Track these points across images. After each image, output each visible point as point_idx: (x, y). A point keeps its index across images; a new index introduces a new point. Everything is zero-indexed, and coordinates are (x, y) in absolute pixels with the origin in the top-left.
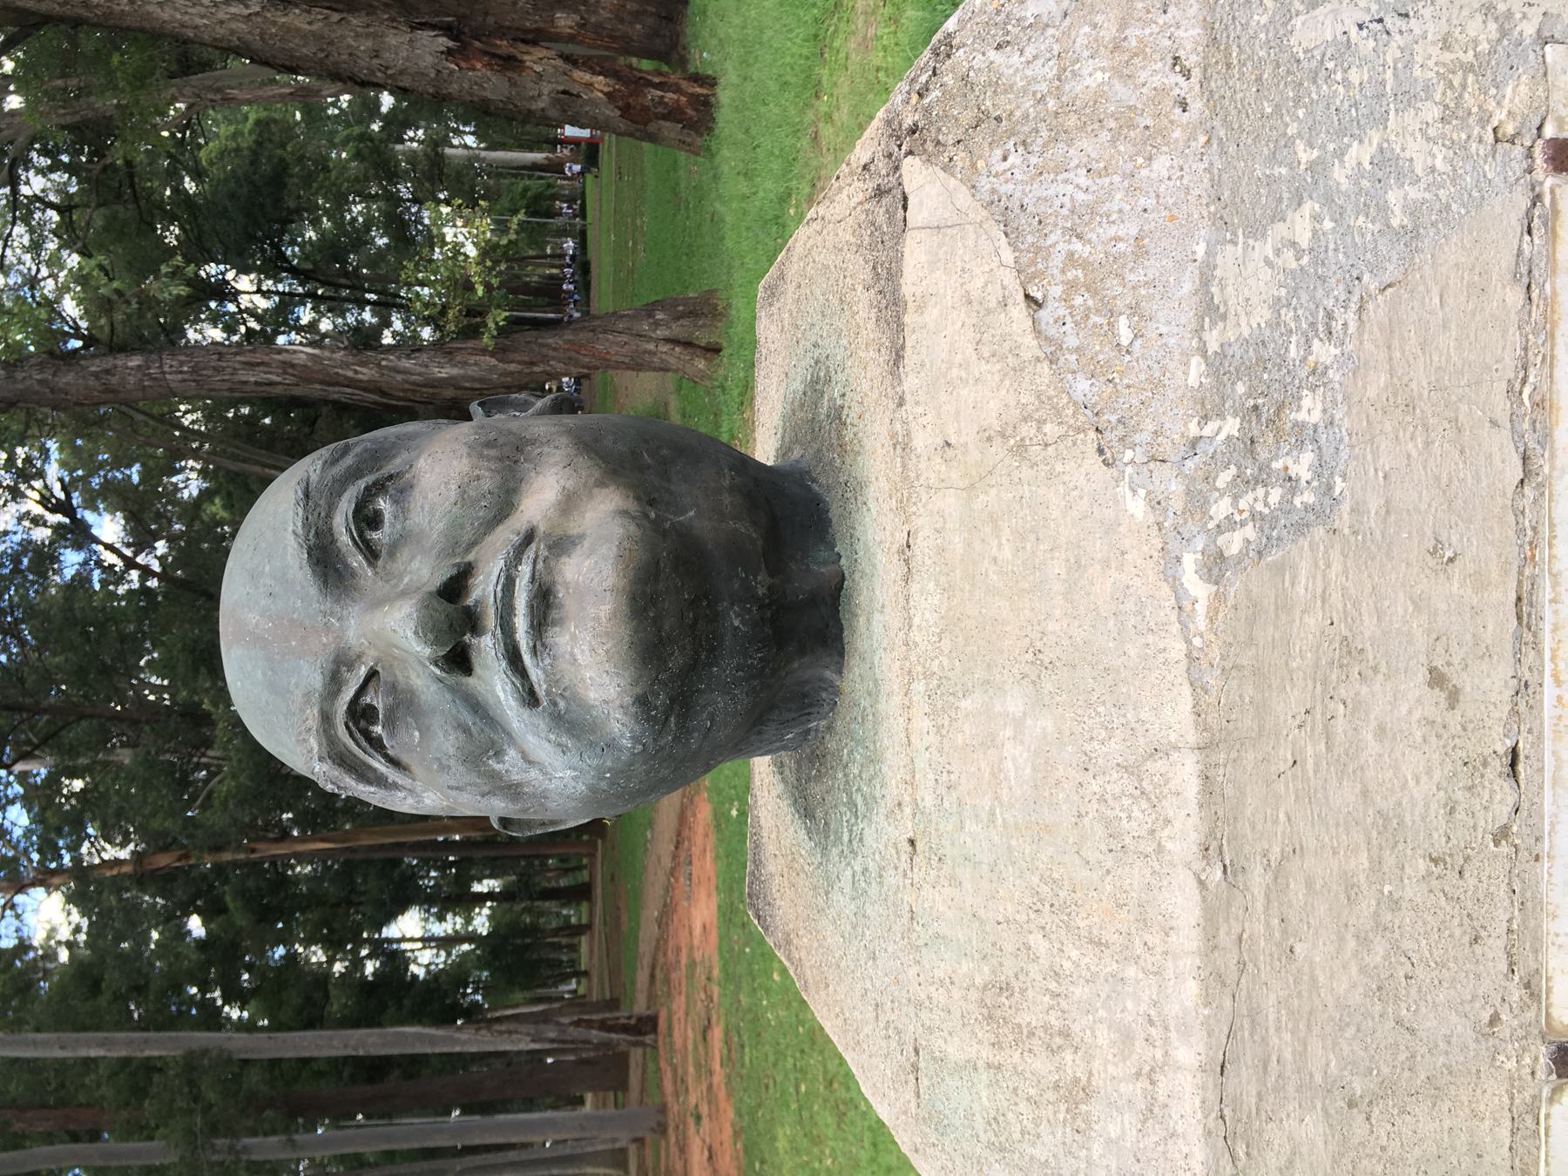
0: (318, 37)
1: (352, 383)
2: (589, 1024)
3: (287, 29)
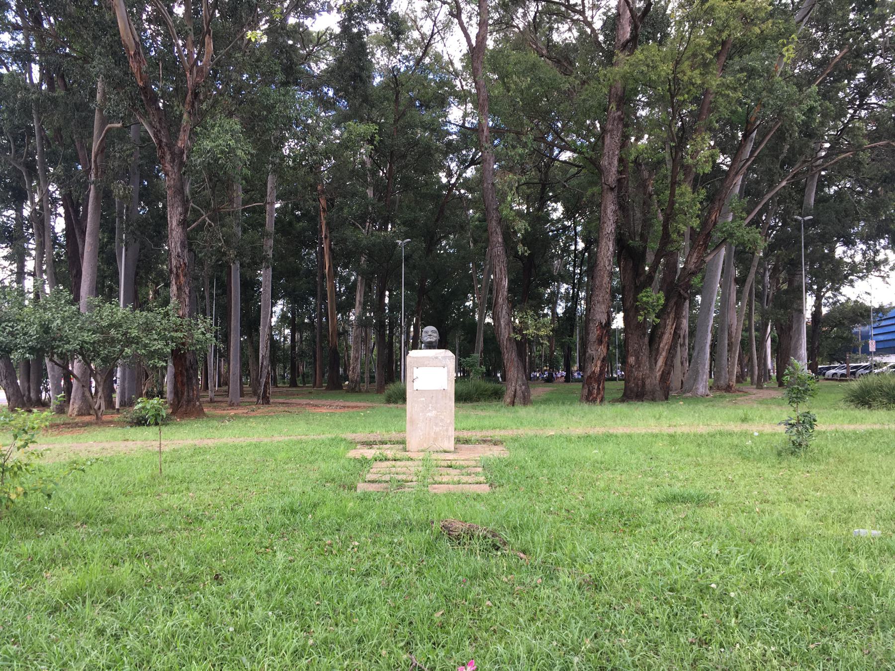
0: (602, 285)
1: (497, 297)
2: (267, 378)
3: (603, 277)
